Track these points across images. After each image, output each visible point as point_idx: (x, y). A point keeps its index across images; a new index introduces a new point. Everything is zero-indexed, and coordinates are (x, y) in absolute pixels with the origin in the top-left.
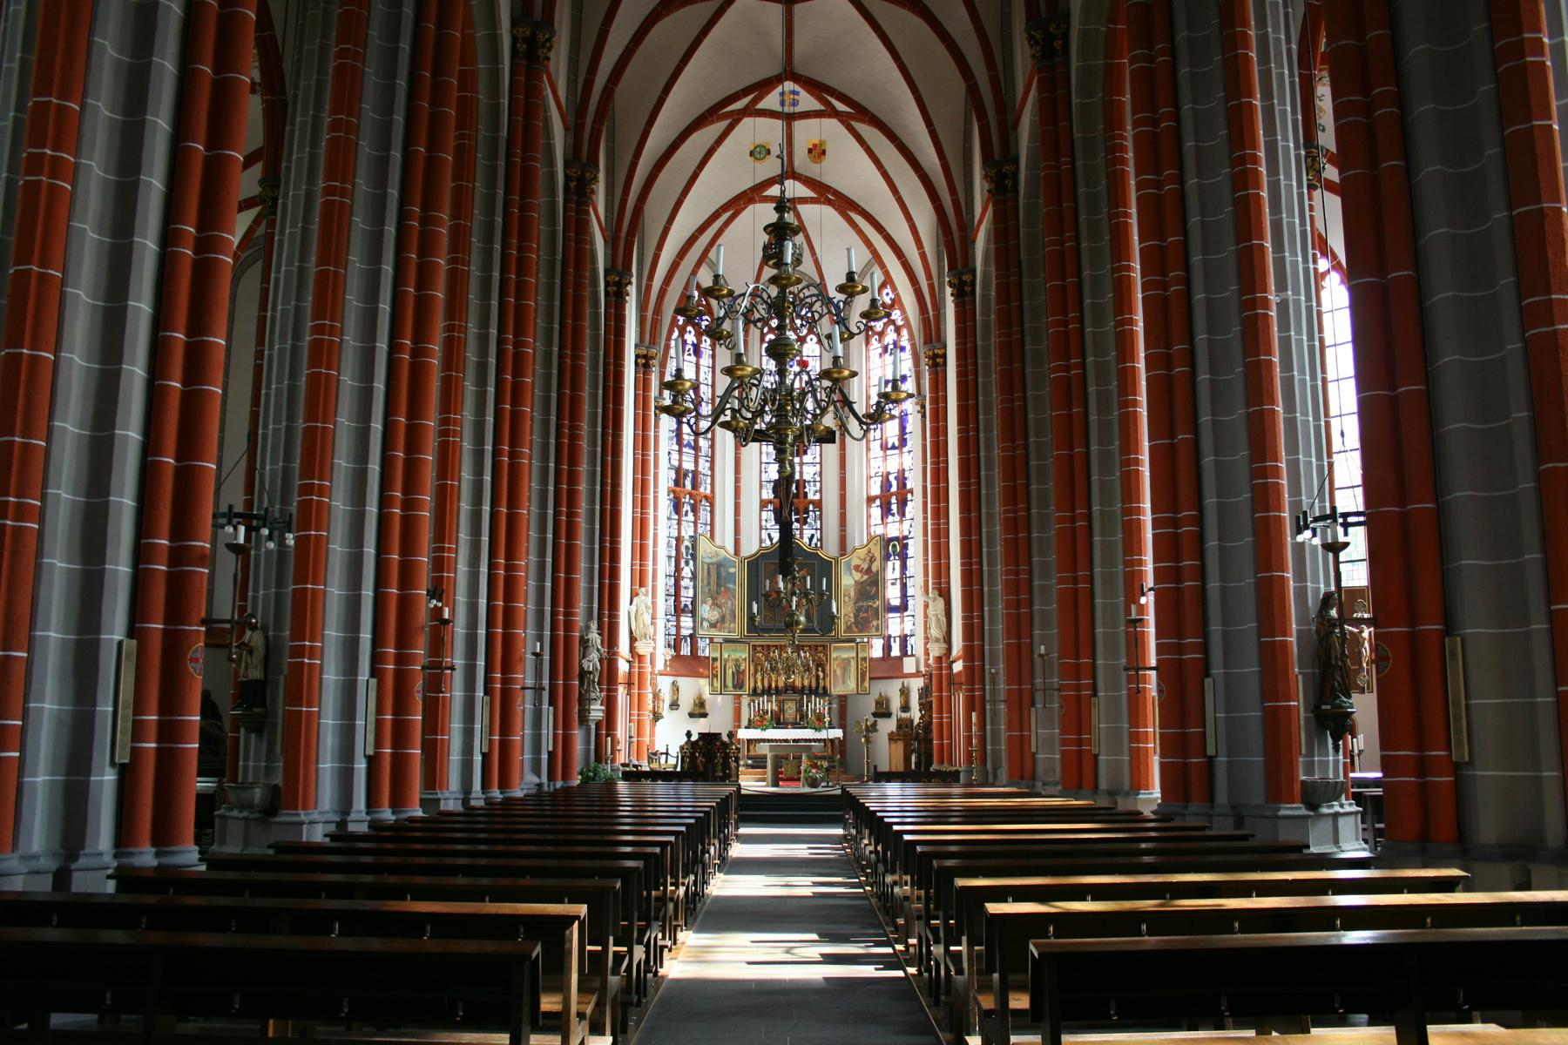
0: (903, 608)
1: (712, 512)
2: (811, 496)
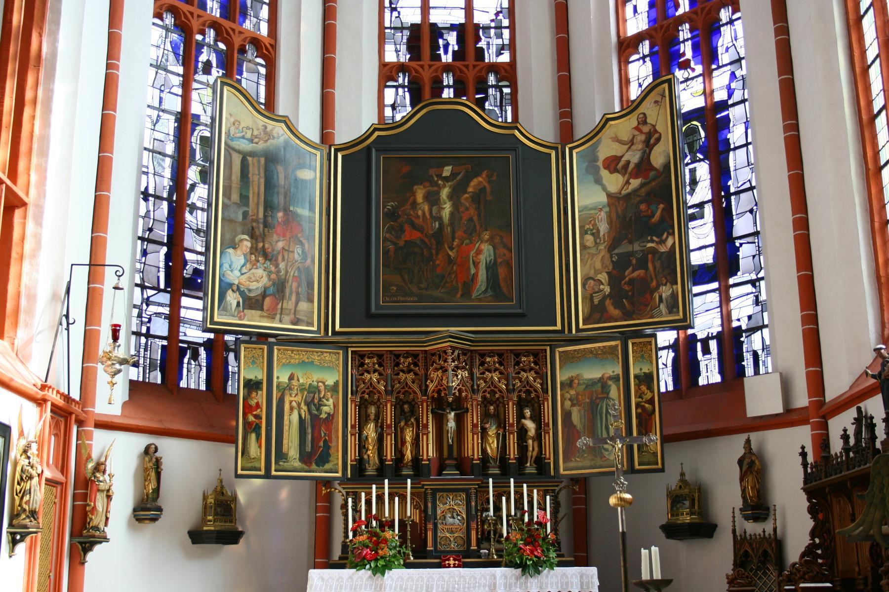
1: (271, 79)
2: (491, 57)
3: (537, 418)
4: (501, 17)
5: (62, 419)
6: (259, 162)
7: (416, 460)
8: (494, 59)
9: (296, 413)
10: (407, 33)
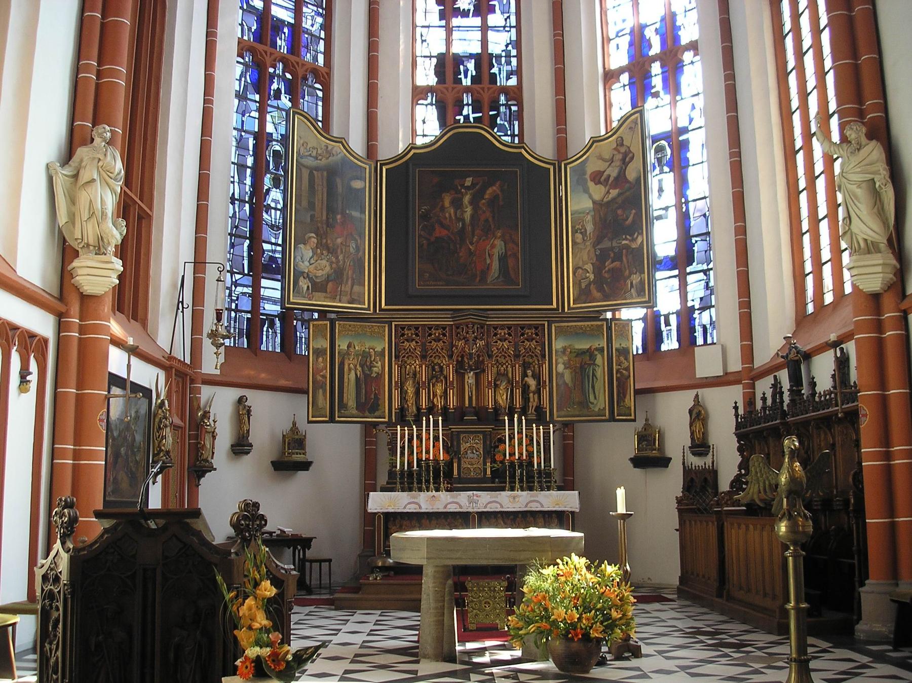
1: (326, 101)
2: (501, 81)
3: (537, 377)
4: (510, 47)
5: (180, 380)
6: (322, 175)
7: (445, 409)
8: (504, 83)
9: (353, 372)
10: (434, 61)
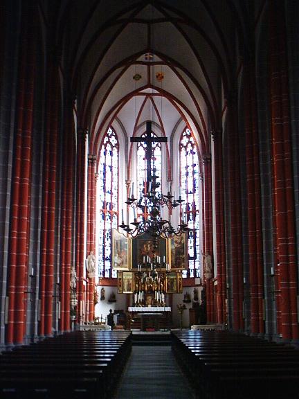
0: (195, 258)
3: (163, 284)
